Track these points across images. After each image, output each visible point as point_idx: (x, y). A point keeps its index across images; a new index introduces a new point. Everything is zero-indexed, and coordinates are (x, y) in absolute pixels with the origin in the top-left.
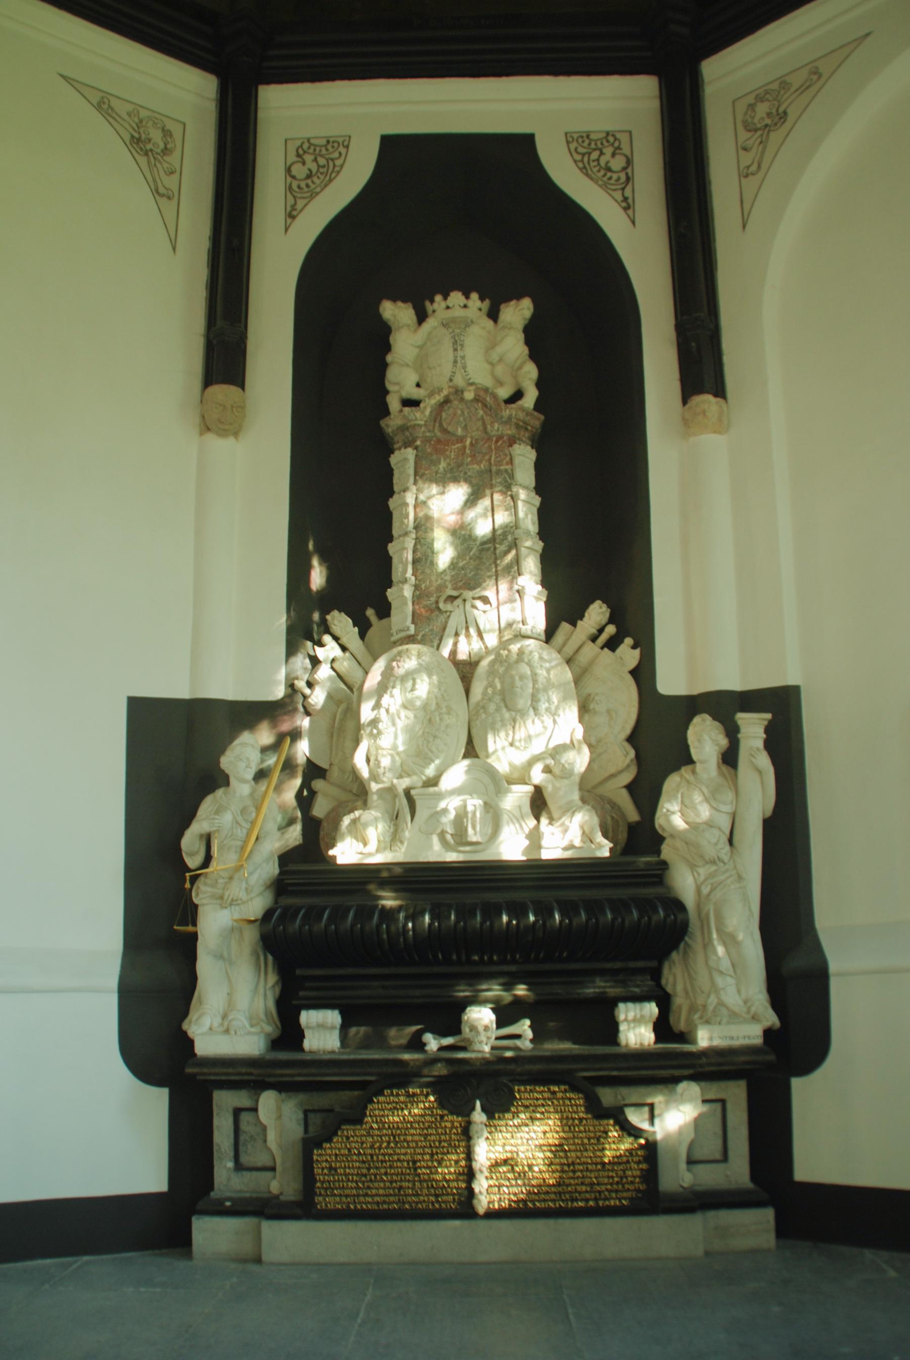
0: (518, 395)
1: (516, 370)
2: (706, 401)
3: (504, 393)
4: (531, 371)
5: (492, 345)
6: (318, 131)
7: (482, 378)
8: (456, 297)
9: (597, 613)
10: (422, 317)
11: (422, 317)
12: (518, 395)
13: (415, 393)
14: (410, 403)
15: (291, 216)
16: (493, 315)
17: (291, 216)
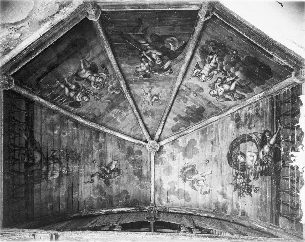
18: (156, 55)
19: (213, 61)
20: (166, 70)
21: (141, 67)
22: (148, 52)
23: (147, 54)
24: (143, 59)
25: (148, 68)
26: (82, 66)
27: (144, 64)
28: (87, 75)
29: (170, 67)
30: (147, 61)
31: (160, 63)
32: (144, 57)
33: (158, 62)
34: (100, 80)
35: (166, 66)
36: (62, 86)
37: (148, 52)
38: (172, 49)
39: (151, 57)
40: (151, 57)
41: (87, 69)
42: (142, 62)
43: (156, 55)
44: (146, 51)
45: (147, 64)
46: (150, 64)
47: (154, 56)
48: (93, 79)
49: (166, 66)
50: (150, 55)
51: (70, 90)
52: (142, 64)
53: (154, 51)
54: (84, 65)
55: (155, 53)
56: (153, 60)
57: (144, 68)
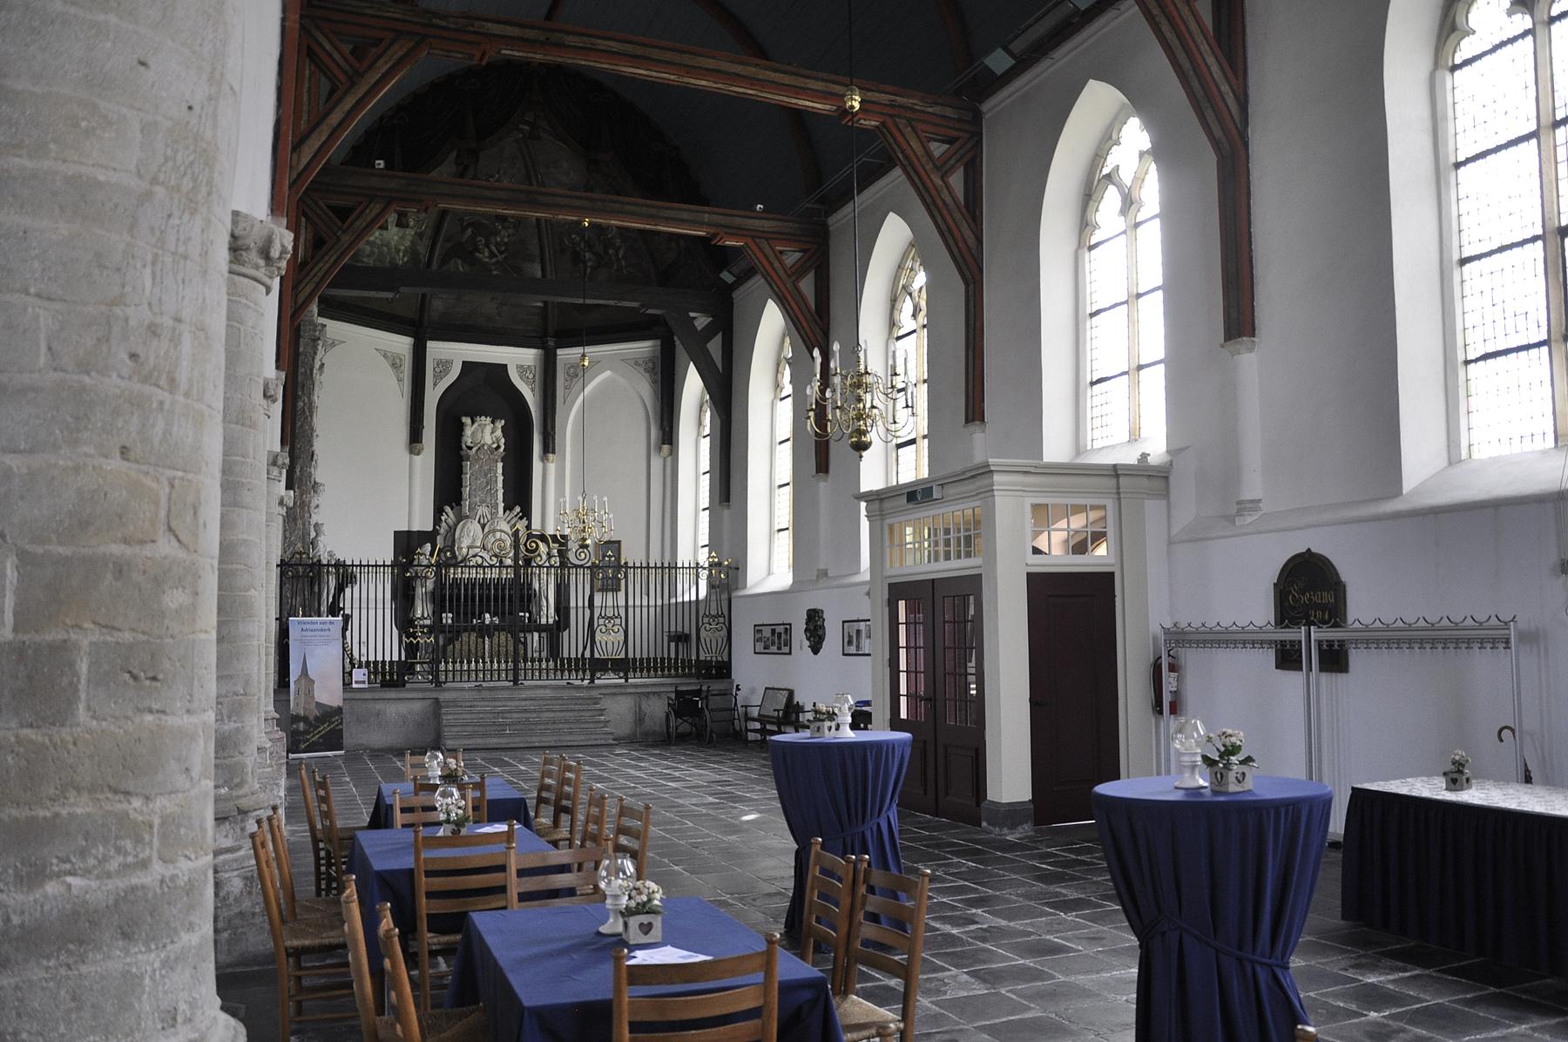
0: (499, 447)
1: (498, 440)
2: (551, 456)
3: (495, 446)
4: (503, 440)
5: (492, 433)
6: (443, 357)
7: (490, 442)
8: (483, 418)
9: (518, 509)
10: (473, 422)
11: (473, 422)
12: (499, 447)
13: (469, 444)
14: (470, 448)
15: (435, 385)
16: (493, 422)
17: (435, 385)
18: (482, 253)
19: (401, 254)
20: (470, 225)
21: (508, 236)
22: (494, 260)
23: (496, 256)
24: (503, 248)
25: (497, 233)
26: (589, 270)
27: (502, 239)
28: (587, 255)
29: (464, 229)
30: (497, 245)
31: (479, 239)
32: (501, 253)
33: (481, 240)
34: (574, 236)
35: (469, 232)
36: (623, 263)
37: (494, 260)
38: (459, 261)
39: (491, 251)
40: (491, 251)
41: (585, 263)
42: (506, 244)
43: (482, 253)
44: (498, 261)
45: (499, 239)
46: (493, 240)
47: (487, 254)
48: (582, 245)
49: (469, 232)
50: (492, 255)
51: (617, 250)
52: (506, 240)
53: (487, 260)
54: (585, 270)
55: (484, 256)
56: (488, 247)
57: (505, 233)
